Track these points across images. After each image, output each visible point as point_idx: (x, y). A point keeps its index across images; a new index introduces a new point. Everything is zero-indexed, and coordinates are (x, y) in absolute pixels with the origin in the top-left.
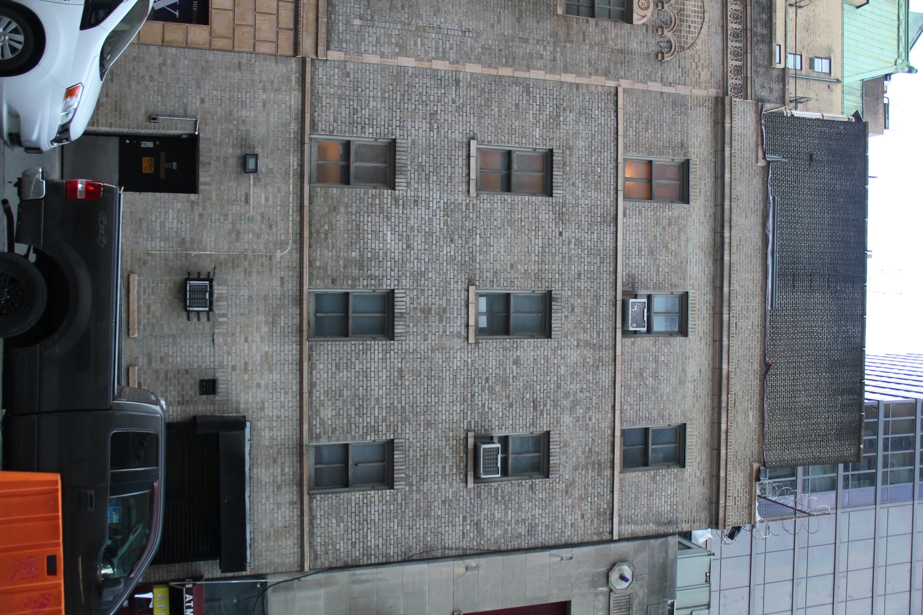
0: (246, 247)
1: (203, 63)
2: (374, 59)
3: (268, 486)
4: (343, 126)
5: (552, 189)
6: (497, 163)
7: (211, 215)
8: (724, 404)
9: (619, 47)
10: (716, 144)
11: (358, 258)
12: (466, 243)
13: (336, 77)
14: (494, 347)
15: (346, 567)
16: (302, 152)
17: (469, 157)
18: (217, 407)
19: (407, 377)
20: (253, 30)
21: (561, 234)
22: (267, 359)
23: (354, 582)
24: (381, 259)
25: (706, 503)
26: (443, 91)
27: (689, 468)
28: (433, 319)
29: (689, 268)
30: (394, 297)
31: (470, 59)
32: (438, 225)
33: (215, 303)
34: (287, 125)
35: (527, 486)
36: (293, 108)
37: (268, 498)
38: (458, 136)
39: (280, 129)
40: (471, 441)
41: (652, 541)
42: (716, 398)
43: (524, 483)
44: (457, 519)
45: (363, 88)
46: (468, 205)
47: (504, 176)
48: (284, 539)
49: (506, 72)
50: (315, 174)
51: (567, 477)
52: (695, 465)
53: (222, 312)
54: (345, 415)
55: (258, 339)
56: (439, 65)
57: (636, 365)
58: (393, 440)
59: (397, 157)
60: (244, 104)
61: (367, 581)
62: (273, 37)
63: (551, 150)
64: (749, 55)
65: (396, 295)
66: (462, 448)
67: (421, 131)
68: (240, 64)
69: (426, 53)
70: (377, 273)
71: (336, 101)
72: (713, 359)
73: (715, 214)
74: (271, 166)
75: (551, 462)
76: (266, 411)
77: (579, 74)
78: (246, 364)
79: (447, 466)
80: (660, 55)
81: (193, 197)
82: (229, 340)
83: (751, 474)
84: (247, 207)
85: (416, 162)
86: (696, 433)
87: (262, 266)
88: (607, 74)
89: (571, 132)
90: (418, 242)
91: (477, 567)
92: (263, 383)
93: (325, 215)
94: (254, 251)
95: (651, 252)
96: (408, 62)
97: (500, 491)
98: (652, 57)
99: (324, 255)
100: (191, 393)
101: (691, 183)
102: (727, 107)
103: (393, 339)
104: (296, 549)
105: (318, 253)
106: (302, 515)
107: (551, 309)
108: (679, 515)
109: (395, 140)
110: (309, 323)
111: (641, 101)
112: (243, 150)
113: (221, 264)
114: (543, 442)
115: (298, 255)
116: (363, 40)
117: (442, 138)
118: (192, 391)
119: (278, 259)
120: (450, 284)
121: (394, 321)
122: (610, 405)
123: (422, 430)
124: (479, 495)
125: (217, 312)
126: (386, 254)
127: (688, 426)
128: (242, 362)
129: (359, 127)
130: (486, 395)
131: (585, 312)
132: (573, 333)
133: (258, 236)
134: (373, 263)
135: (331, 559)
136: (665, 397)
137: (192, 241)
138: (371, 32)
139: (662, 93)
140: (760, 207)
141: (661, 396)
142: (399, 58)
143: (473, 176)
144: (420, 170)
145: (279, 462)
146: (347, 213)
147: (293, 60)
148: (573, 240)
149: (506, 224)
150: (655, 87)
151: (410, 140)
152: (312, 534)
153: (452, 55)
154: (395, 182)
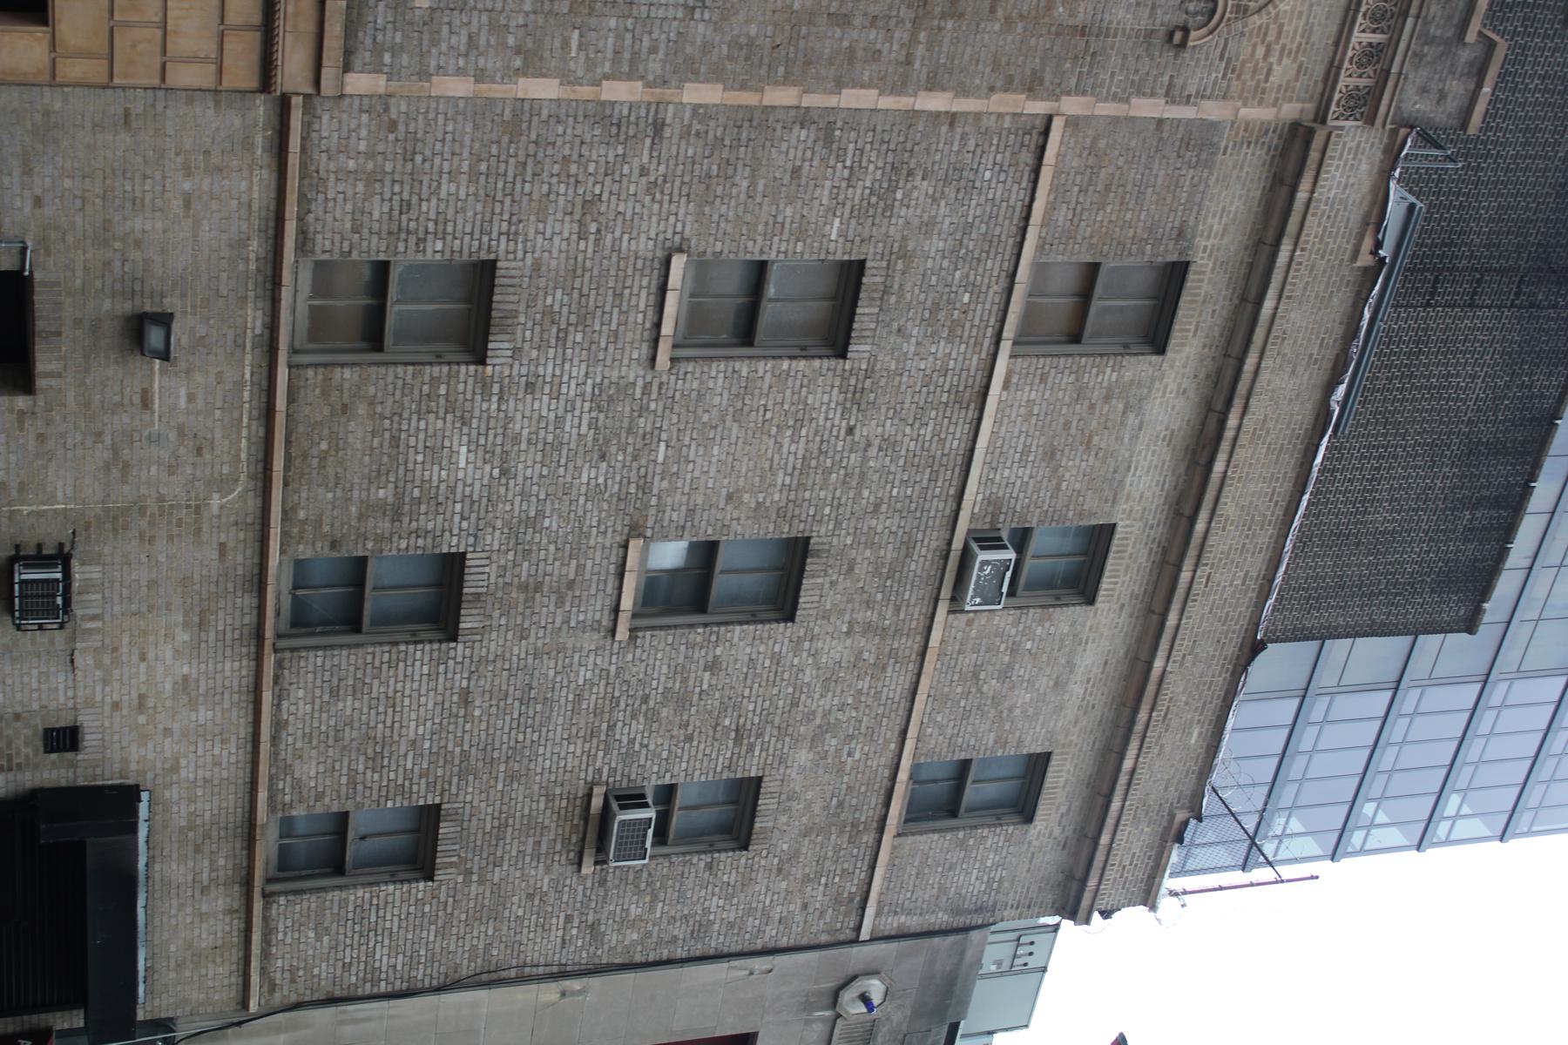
0: (144, 490)
1: (38, 117)
2: (458, 87)
3: (182, 888)
4: (375, 239)
5: (847, 343)
6: (731, 285)
7: (63, 435)
8: (1139, 727)
9: (1080, 19)
10: (1266, 227)
11: (390, 499)
12: (635, 458)
13: (364, 133)
14: (665, 653)
15: (332, 1001)
16: (275, 301)
17: (663, 289)
18: (80, 771)
19: (477, 703)
20: (159, 33)
21: (850, 430)
22: (185, 689)
23: (342, 1023)
24: (441, 499)
25: (1061, 877)
26: (620, 150)
27: (1039, 824)
28: (546, 607)
29: (1128, 480)
30: (463, 566)
31: (696, 72)
32: (577, 427)
33: (75, 598)
34: (243, 243)
35: (702, 864)
36: (255, 206)
37: (181, 906)
38: (644, 246)
39: (225, 253)
40: (597, 802)
41: (937, 940)
42: (1127, 712)
43: (695, 860)
44: (554, 921)
45: (428, 153)
46: (647, 387)
47: (740, 318)
48: (210, 966)
49: (782, 96)
50: (302, 332)
51: (785, 847)
52: (1055, 818)
53: (91, 611)
54: (345, 771)
55: (169, 654)
56: (620, 92)
57: (968, 660)
58: (439, 805)
59: (496, 298)
60: (137, 204)
61: (369, 1019)
62: (208, 47)
63: (861, 264)
64: (1410, 21)
65: (468, 563)
66: (577, 811)
67: (557, 240)
68: (127, 114)
69: (591, 65)
70: (430, 526)
71: (360, 187)
72: (1139, 641)
73: (1219, 371)
74: (201, 330)
75: (757, 825)
76: (183, 773)
77: (962, 91)
78: (142, 697)
79: (545, 839)
80: (1178, 36)
81: (22, 402)
82: (107, 659)
83: (1167, 829)
84: (146, 417)
85: (540, 308)
86: (1069, 766)
87: (179, 525)
88: (1032, 87)
89: (916, 222)
90: (527, 466)
91: (582, 991)
92: (176, 726)
93: (321, 423)
94: (161, 499)
95: (1051, 454)
96: (543, 89)
97: (645, 875)
98: (1157, 41)
99: (315, 500)
100: (29, 750)
101: (1180, 313)
102: (1314, 155)
103: (455, 639)
104: (233, 980)
105: (304, 495)
106: (248, 931)
107: (802, 570)
108: (1001, 897)
109: (491, 266)
110: (278, 613)
111: (1102, 143)
112: (137, 302)
113: (87, 527)
114: (744, 796)
115: (259, 501)
116: (435, 42)
117: (607, 252)
118: (25, 744)
119: (215, 510)
120: (588, 537)
121: (459, 608)
122: (897, 729)
123: (500, 787)
124: (603, 882)
125: (78, 611)
126: (453, 491)
127: (1054, 757)
128: (134, 695)
129: (413, 239)
130: (638, 725)
131: (877, 573)
132: (841, 612)
133: (172, 470)
134: (423, 508)
135: (302, 990)
136: (1017, 712)
137: (22, 487)
138: (457, 22)
139: (1160, 122)
140: (1330, 354)
141: (1010, 710)
142: (521, 80)
143: (667, 328)
144: (547, 321)
145: (207, 850)
146: (372, 415)
147: (260, 99)
148: (877, 442)
149: (729, 419)
150: (1147, 108)
151: (529, 261)
152: (266, 955)
153: (655, 66)
154: (486, 349)
